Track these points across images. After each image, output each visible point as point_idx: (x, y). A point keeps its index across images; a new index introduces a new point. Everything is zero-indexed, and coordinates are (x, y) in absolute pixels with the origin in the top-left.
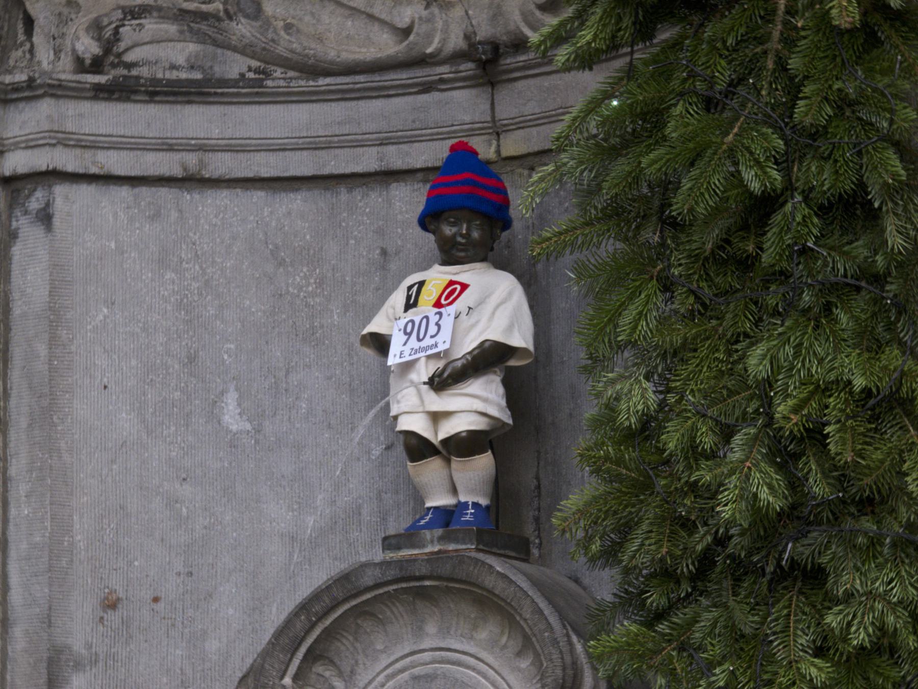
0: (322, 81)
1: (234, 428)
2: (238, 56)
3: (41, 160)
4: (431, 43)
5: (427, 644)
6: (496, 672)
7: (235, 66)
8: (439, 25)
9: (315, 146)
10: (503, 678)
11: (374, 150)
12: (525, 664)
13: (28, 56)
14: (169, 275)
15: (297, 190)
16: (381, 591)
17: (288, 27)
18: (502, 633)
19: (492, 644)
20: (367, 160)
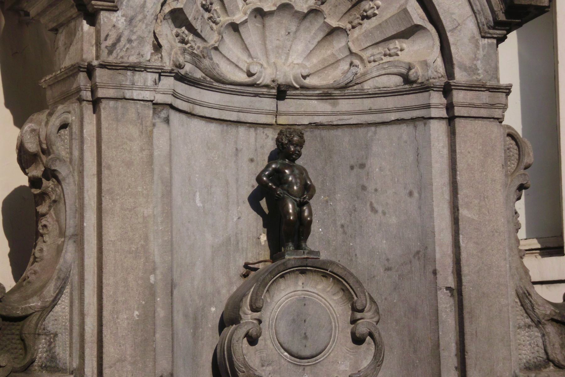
0: (228, 86)
1: (198, 205)
2: (200, 71)
3: (169, 99)
4: (259, 80)
5: (300, 288)
6: (325, 300)
7: (199, 75)
8: (263, 75)
9: (221, 108)
10: (328, 302)
11: (235, 114)
12: (335, 298)
13: (160, 59)
14: (185, 147)
15: (212, 123)
16: (292, 269)
17: (218, 65)
18: (329, 287)
19: (324, 290)
20: (233, 116)
